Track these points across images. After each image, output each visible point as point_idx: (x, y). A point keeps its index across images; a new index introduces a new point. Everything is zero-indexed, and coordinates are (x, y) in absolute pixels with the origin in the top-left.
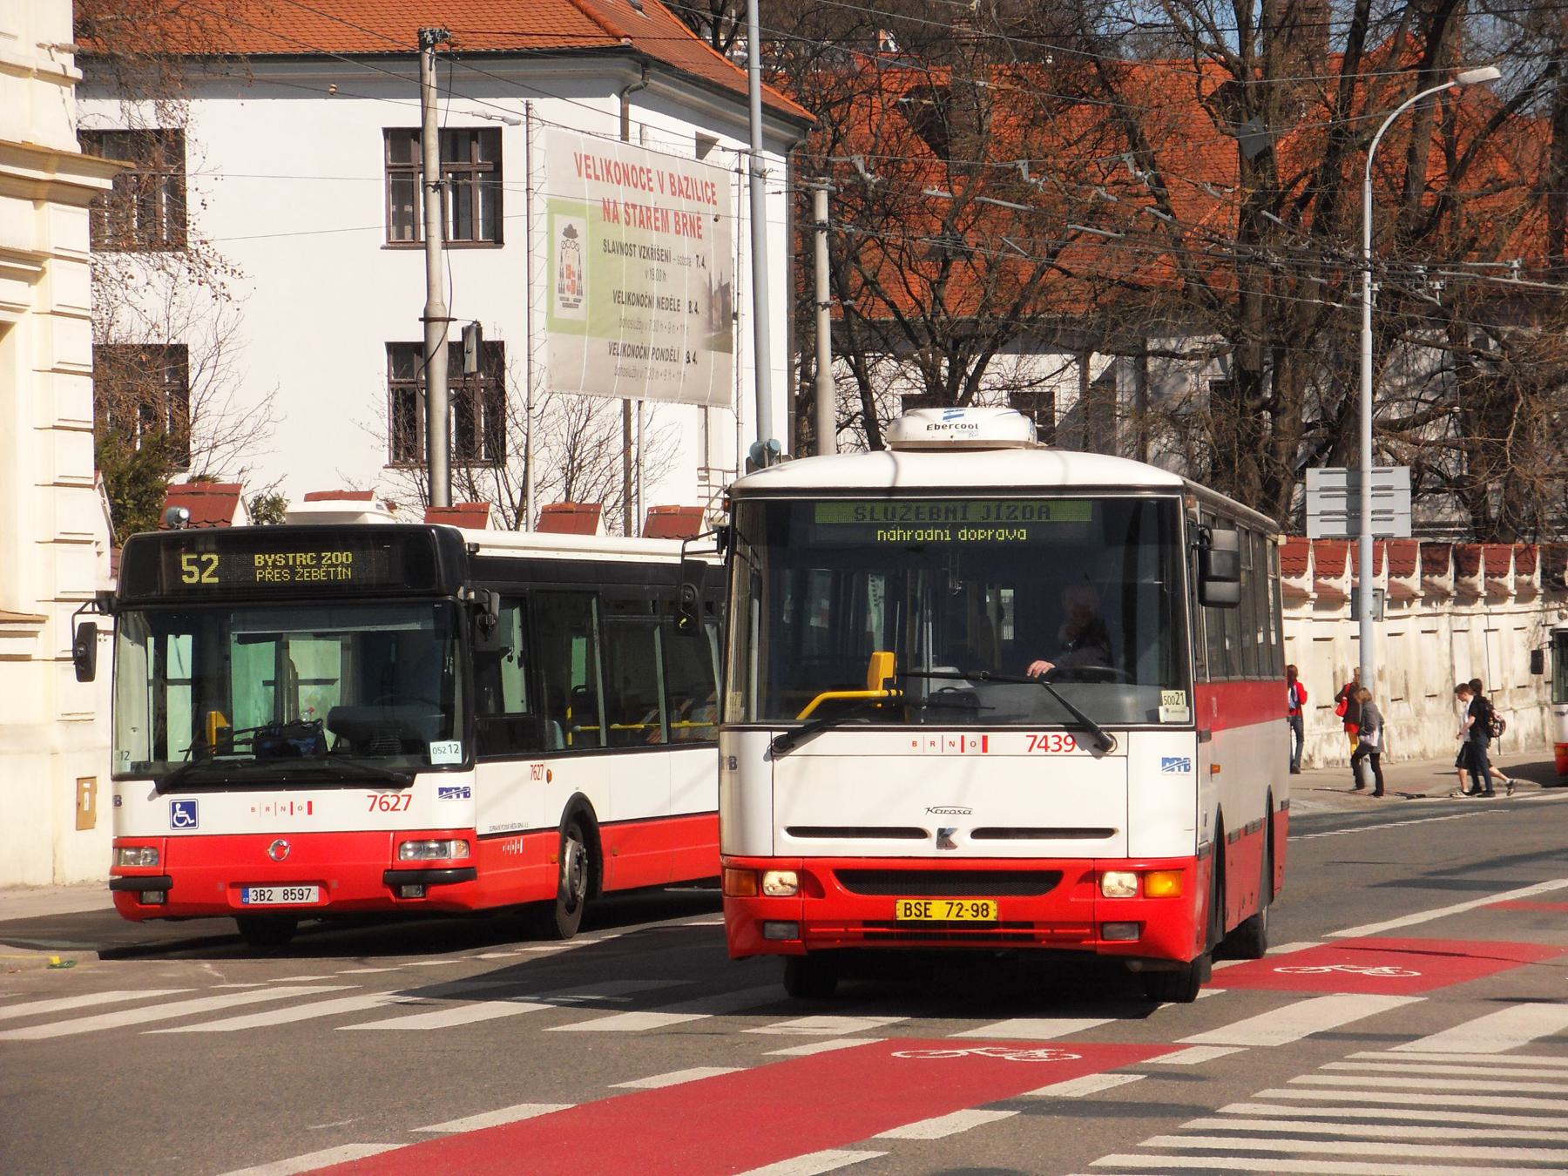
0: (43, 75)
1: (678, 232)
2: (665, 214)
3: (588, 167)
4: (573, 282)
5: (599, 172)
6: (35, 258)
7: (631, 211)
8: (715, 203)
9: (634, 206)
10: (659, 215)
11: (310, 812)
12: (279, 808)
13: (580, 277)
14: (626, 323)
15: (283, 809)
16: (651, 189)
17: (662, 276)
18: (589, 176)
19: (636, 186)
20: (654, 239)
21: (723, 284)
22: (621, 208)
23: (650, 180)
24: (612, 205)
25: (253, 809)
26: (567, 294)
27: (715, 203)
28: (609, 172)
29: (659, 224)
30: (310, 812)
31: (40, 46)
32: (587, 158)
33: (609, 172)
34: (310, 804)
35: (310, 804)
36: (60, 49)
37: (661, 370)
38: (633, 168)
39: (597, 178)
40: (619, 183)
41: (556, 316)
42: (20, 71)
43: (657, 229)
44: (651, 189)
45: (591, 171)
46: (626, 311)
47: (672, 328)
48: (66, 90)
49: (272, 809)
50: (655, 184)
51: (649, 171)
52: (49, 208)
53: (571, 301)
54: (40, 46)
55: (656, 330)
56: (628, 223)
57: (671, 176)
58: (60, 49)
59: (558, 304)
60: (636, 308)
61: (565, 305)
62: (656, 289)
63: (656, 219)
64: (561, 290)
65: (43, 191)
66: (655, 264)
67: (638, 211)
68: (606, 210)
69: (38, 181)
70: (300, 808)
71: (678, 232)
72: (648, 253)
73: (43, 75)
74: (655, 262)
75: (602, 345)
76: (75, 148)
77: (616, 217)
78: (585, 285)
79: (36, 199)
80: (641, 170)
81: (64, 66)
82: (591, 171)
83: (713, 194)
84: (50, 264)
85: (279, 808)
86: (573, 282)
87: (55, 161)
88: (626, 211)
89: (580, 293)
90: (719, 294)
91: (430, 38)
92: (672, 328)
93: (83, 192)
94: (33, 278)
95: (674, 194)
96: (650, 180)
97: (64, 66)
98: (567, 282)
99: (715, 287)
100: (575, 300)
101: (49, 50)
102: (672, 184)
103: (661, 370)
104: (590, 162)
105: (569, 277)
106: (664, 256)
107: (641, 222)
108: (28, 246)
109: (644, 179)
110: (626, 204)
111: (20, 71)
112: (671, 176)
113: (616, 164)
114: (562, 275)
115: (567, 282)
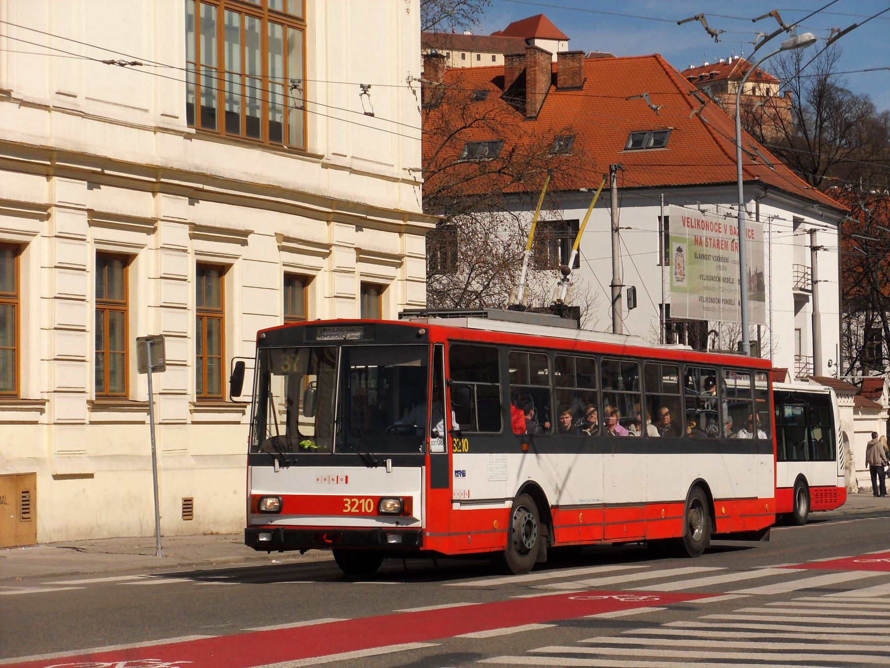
0: (405, 181)
1: (732, 250)
2: (726, 244)
3: (688, 222)
4: (681, 270)
5: (693, 225)
6: (400, 257)
7: (709, 241)
8: (753, 238)
9: (711, 239)
10: (723, 243)
11: (347, 482)
12: (331, 480)
13: (684, 269)
14: (707, 288)
15: (333, 480)
16: (720, 232)
17: (725, 269)
18: (688, 226)
19: (712, 230)
20: (721, 253)
21: (758, 272)
22: (704, 239)
23: (720, 228)
24: (699, 237)
25: (318, 479)
26: (678, 276)
27: (753, 238)
28: (698, 224)
29: (723, 246)
30: (347, 482)
31: (404, 169)
32: (688, 218)
33: (698, 224)
34: (347, 477)
35: (347, 477)
36: (414, 170)
37: (727, 308)
38: (711, 223)
39: (692, 227)
40: (703, 229)
41: (674, 285)
42: (395, 180)
43: (722, 249)
44: (720, 232)
45: (689, 224)
46: (706, 283)
47: (730, 291)
48: (417, 188)
49: (327, 480)
50: (722, 230)
51: (720, 224)
52: (406, 236)
53: (680, 279)
54: (404, 169)
55: (723, 291)
56: (707, 246)
57: (731, 226)
58: (414, 170)
59: (675, 280)
60: (711, 283)
61: (677, 280)
62: (722, 274)
63: (722, 244)
64: (676, 274)
65: (403, 229)
66: (721, 264)
67: (712, 241)
68: (696, 240)
69: (401, 225)
70: (342, 480)
71: (732, 250)
72: (719, 259)
73: (405, 181)
74: (721, 263)
75: (695, 298)
76: (419, 210)
77: (701, 243)
78: (686, 272)
79: (401, 233)
80: (716, 224)
81: (415, 177)
82: (689, 224)
83: (752, 234)
84: (406, 260)
85: (331, 480)
86: (681, 270)
87: (407, 217)
88: (707, 242)
89: (684, 275)
90: (755, 277)
91: (614, 168)
92: (730, 291)
93: (425, 229)
94: (399, 265)
95: (731, 234)
96: (720, 228)
97: (415, 177)
98: (678, 270)
99: (752, 273)
100: (682, 278)
101: (409, 171)
102: (731, 230)
103: (727, 308)
104: (689, 220)
105: (679, 269)
106: (726, 260)
107: (714, 245)
108: (397, 252)
109: (717, 227)
110: (706, 238)
111: (395, 180)
112: (731, 226)
113: (703, 221)
114: (676, 268)
115: (678, 270)
